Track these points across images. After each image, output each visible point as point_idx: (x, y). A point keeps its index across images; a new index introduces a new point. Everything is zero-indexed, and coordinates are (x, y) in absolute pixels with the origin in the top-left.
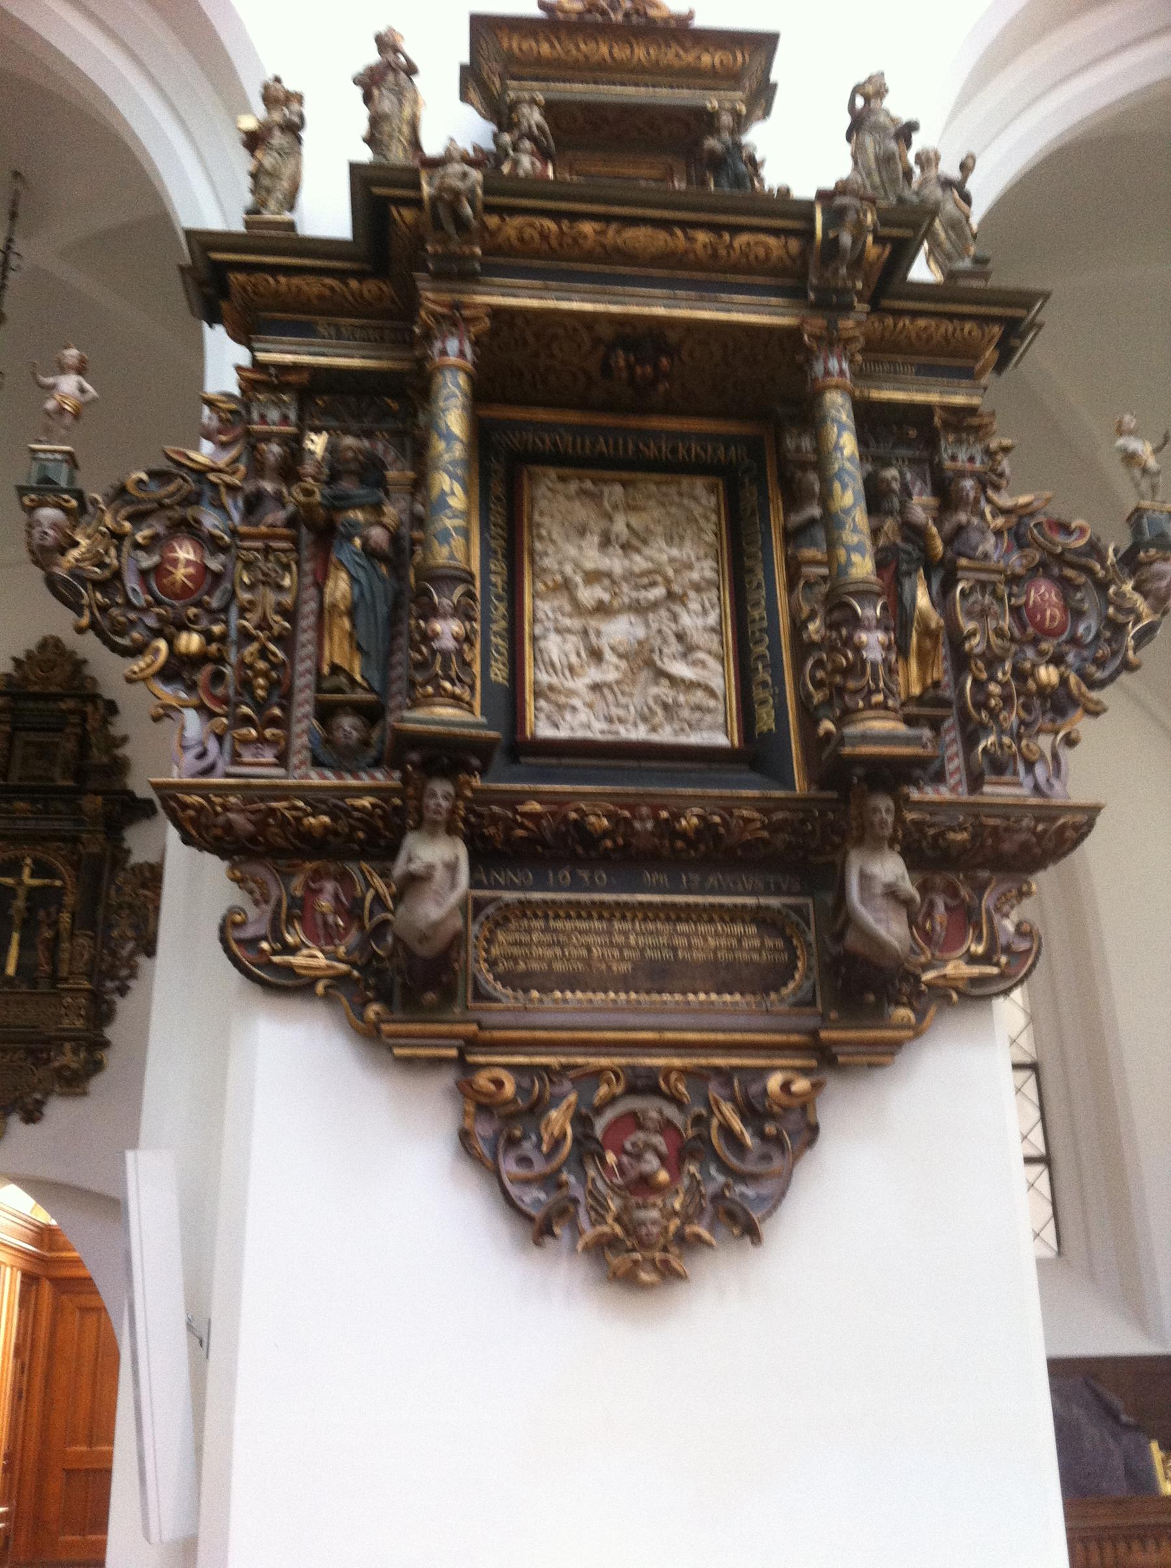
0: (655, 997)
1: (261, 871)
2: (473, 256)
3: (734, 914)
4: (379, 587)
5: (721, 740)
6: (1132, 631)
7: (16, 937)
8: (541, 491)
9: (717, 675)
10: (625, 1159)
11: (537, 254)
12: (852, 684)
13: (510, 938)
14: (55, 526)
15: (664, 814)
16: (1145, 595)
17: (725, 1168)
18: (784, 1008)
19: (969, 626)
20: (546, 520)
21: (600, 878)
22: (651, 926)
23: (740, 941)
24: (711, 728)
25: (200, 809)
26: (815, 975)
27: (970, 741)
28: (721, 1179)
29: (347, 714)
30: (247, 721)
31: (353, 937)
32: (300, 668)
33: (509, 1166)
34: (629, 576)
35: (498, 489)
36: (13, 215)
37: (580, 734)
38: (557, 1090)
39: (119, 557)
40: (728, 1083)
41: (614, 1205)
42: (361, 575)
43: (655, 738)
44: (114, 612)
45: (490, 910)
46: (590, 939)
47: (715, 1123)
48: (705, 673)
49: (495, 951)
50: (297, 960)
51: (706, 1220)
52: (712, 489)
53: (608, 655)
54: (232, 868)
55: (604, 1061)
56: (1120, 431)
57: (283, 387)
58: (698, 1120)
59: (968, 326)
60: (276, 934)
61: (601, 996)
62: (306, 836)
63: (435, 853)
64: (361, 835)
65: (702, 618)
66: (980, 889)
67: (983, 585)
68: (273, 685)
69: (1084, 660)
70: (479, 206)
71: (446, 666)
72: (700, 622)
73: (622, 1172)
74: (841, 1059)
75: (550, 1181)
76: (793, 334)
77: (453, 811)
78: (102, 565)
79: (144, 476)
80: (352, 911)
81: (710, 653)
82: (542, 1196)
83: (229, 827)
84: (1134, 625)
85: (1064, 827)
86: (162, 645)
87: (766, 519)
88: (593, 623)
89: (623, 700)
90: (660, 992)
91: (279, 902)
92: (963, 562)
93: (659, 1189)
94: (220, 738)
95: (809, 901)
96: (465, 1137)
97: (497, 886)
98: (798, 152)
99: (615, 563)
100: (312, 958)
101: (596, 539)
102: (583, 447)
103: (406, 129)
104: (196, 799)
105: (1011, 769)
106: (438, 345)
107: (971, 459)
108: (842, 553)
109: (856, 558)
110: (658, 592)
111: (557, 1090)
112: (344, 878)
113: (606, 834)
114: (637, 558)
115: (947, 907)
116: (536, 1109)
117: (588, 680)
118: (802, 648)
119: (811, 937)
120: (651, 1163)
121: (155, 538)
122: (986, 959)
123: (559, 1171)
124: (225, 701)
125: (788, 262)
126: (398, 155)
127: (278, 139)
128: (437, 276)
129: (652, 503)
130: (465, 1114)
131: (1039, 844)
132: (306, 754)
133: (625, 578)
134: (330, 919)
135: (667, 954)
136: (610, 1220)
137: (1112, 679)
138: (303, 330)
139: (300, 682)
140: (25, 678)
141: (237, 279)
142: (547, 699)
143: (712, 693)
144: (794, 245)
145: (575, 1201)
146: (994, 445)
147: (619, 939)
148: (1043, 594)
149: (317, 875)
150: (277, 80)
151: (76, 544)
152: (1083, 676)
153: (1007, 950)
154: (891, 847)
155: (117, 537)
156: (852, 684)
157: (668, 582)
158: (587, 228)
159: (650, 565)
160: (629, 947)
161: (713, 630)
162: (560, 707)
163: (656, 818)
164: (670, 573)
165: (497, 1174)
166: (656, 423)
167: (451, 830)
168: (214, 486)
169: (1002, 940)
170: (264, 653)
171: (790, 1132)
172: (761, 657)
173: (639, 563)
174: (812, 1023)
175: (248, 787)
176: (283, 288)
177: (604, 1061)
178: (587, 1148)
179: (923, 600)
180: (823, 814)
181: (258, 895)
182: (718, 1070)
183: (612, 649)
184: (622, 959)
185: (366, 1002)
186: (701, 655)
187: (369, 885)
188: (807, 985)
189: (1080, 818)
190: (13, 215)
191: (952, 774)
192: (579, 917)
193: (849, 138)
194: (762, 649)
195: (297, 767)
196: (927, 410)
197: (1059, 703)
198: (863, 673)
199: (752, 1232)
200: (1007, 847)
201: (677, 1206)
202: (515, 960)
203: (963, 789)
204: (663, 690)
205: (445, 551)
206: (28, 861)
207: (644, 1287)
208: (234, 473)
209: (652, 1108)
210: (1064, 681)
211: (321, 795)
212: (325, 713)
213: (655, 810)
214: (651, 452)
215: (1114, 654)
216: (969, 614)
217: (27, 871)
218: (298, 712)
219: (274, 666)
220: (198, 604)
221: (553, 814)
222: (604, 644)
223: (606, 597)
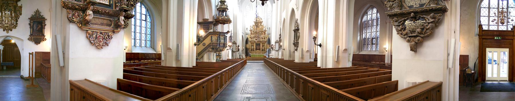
3: (108, 20)
80: (79, 16)
178: (96, 38)
209: (101, 35)
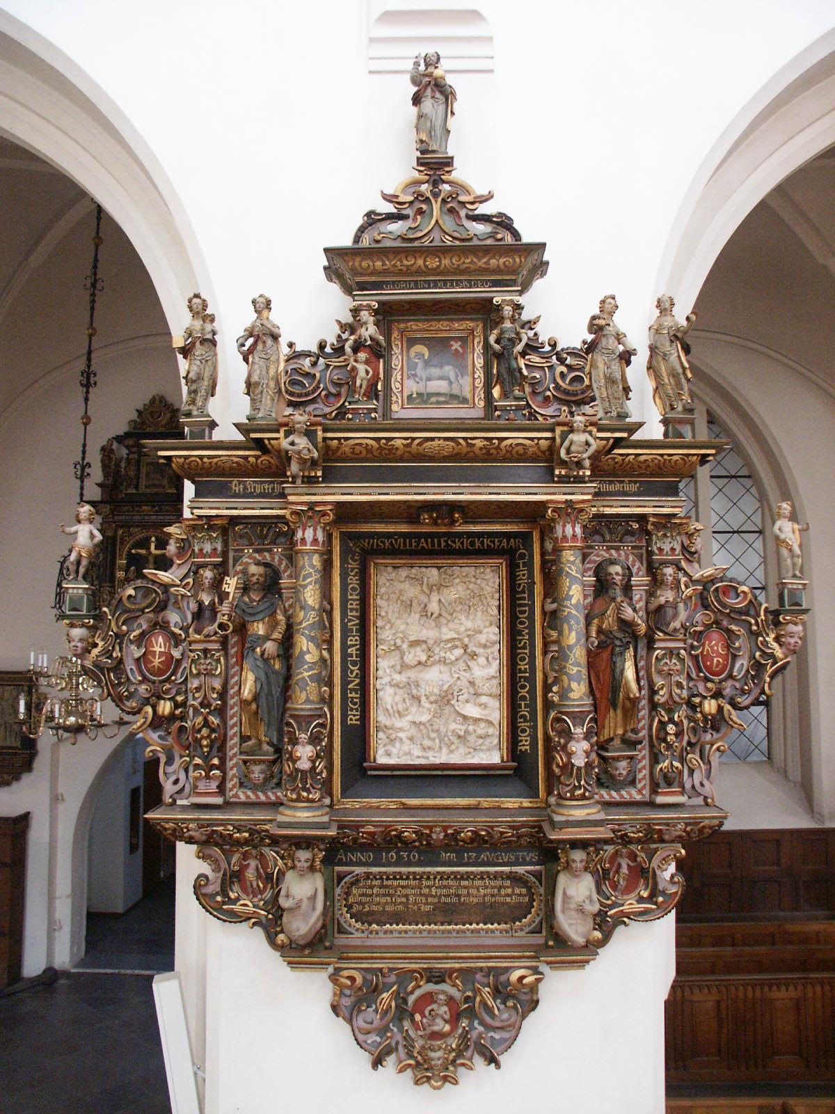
3: (496, 876)
5: (494, 758)
8: (382, 580)
9: (494, 711)
13: (360, 891)
15: (449, 832)
17: (482, 1023)
21: (414, 856)
23: (499, 891)
25: (175, 830)
28: (481, 1029)
34: (438, 642)
38: (387, 980)
39: (121, 650)
46: (408, 891)
47: (478, 999)
49: (351, 900)
57: (211, 528)
60: (224, 893)
65: (488, 670)
71: (304, 781)
73: (424, 1029)
75: (382, 1031)
76: (543, 505)
78: (110, 657)
84: (773, 664)
85: (704, 827)
86: (149, 709)
97: (351, 863)
99: (428, 633)
102: (411, 545)
103: (272, 384)
109: (574, 685)
110: (458, 652)
111: (387, 980)
117: (409, 718)
127: (199, 350)
132: (235, 780)
134: (255, 885)
135: (454, 900)
140: (143, 423)
143: (490, 723)
147: (426, 891)
151: (96, 645)
155: (119, 637)
157: (465, 647)
159: (455, 636)
160: (432, 896)
164: (466, 640)
169: (660, 887)
170: (206, 723)
172: (523, 698)
177: (413, 966)
178: (402, 1012)
179: (630, 673)
184: (427, 904)
186: (484, 699)
188: (538, 920)
189: (716, 822)
192: (401, 878)
195: (231, 790)
197: (717, 722)
201: (454, 1046)
202: (363, 904)
203: (646, 792)
205: (303, 696)
206: (153, 539)
210: (720, 709)
213: (445, 829)
214: (457, 545)
216: (660, 672)
217: (153, 546)
223: (423, 658)
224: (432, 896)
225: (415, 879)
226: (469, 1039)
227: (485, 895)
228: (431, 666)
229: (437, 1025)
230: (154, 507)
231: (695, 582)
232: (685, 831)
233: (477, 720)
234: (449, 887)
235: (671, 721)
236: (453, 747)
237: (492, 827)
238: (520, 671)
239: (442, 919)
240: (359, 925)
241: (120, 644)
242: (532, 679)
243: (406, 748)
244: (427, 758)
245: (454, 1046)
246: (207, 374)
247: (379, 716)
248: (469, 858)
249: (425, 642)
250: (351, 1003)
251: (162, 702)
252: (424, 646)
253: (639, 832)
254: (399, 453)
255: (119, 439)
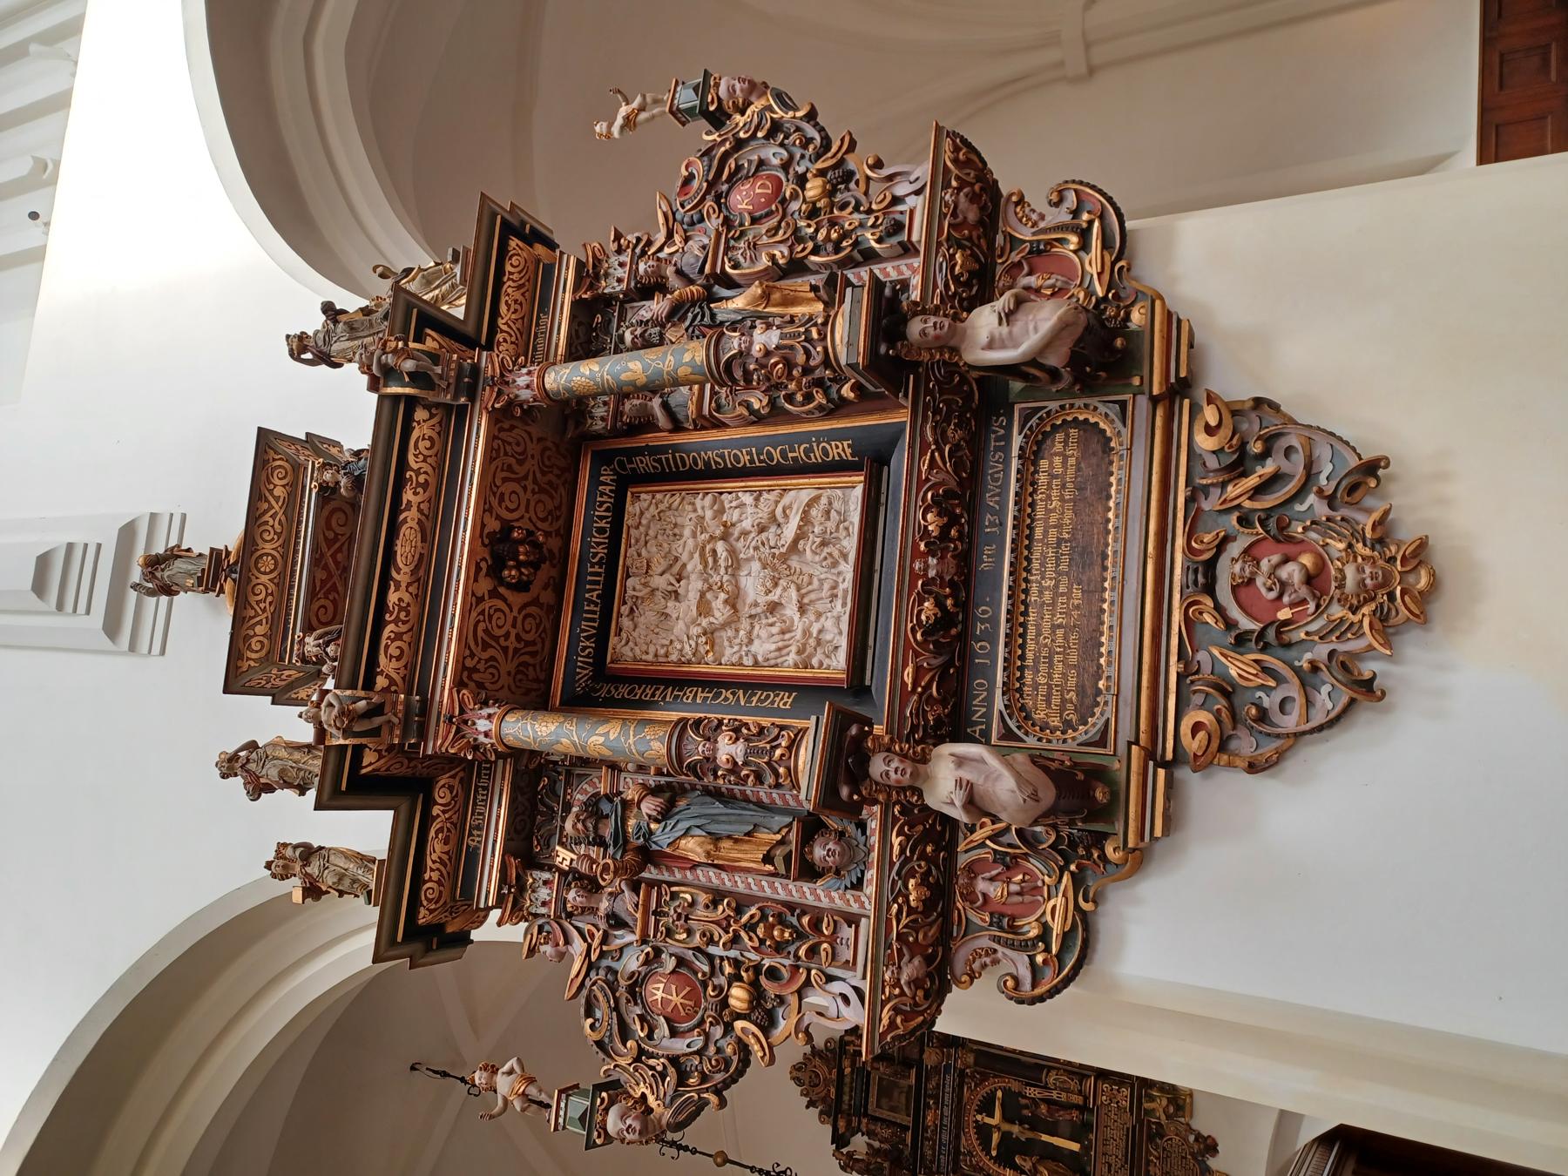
0: (1109, 562)
1: (961, 956)
2: (408, 704)
3: (1027, 481)
4: (694, 810)
6: (779, 113)
7: (1045, 1138)
8: (626, 651)
9: (800, 492)
10: (1286, 599)
11: (414, 645)
12: (800, 358)
13: (1042, 705)
14: (623, 1117)
16: (747, 104)
17: (1299, 495)
18: (1126, 433)
19: (764, 261)
20: (652, 649)
21: (984, 612)
22: (1035, 565)
23: (1056, 477)
24: (846, 502)
25: (895, 1009)
26: (1093, 401)
27: (870, 256)
28: (1312, 499)
29: (811, 853)
30: (813, 951)
31: (1034, 865)
32: (768, 892)
33: (1290, 722)
34: (705, 575)
35: (624, 691)
36: (445, 1074)
37: (845, 627)
38: (1206, 668)
39: (657, 1057)
40: (1205, 490)
41: (1337, 611)
42: (683, 826)
43: (852, 556)
44: (706, 1067)
45: (1012, 724)
46: (1046, 626)
47: (1247, 504)
48: (795, 507)
49: (1055, 722)
50: (1057, 928)
51: (1360, 517)
52: (636, 497)
53: (774, 596)
54: (959, 983)
55: (1177, 617)
56: (609, 135)
57: (521, 887)
58: (1244, 521)
59: (508, 268)
60: (1026, 946)
61: (1106, 617)
62: (928, 905)
63: (946, 778)
64: (929, 849)
65: (745, 505)
66: (1013, 242)
67: (728, 249)
68: (781, 920)
69: (803, 157)
70: (361, 693)
72: (750, 510)
73: (1304, 602)
74: (1183, 375)
75: (1308, 678)
76: (497, 417)
77: (903, 756)
78: (663, 1075)
79: (590, 1021)
81: (777, 502)
82: (1325, 689)
83: (915, 983)
85: (955, 161)
87: (663, 449)
88: (745, 611)
89: (816, 583)
90: (1104, 556)
91: (995, 939)
92: (707, 269)
93: (1321, 566)
94: (831, 979)
95: (1017, 407)
96: (1253, 768)
97: (988, 716)
98: (344, 408)
99: (693, 587)
100: (1056, 910)
101: (671, 604)
102: (594, 612)
103: (297, 755)
104: (886, 1015)
105: (898, 217)
106: (482, 738)
107: (622, 265)
108: (682, 371)
109: (687, 358)
110: (720, 547)
111: (1206, 668)
112: (972, 870)
113: (939, 604)
114: (689, 567)
115: (1030, 274)
116: (1227, 690)
118: (776, 414)
119: (1053, 405)
120: (1292, 572)
121: (642, 1018)
122: (1084, 234)
123: (1297, 671)
124: (795, 969)
125: (435, 420)
126: (315, 765)
128: (423, 735)
129: (644, 552)
130: (1229, 765)
131: (972, 185)
133: (706, 580)
134: (1014, 888)
136: (1356, 618)
137: (821, 130)
138: (473, 858)
139: (782, 896)
140: (824, 1100)
141: (423, 917)
142: (810, 656)
143: (816, 499)
144: (420, 414)
145: (1332, 654)
146: (614, 247)
147: (1047, 596)
148: (742, 200)
149: (970, 897)
150: (268, 866)
152: (818, 156)
153: (1076, 213)
154: (963, 321)
156: (800, 358)
158: (393, 597)
159: (697, 555)
160: (1056, 586)
161: (757, 499)
162: (819, 642)
163: (924, 555)
164: (705, 537)
165: (1298, 735)
166: (576, 547)
167: (924, 759)
168: (602, 955)
169: (1067, 218)
170: (750, 928)
171: (1257, 431)
172: (783, 454)
173: (694, 565)
174: (1143, 401)
175: (875, 960)
176: (435, 875)
177: (1177, 617)
180: (928, 392)
181: (988, 960)
182: (1189, 501)
183: (768, 592)
184: (1069, 595)
185: (1103, 857)
187: (983, 845)
188: (1102, 409)
189: (947, 144)
190: (445, 1074)
191: (900, 273)
193: (339, 365)
194: (777, 455)
196: (576, 304)
198: (791, 347)
199: (1372, 468)
200: (972, 216)
201: (1342, 546)
202: (1064, 701)
204: (807, 546)
205: (656, 745)
206: (979, 1117)
207: (1435, 583)
208: (592, 936)
210: (822, 173)
211: (887, 886)
212: (810, 872)
213: (916, 554)
214: (602, 551)
215: (798, 129)
217: (988, 1120)
218: (810, 900)
219: (764, 917)
220: (705, 985)
221: (916, 654)
222: (762, 600)
223: (723, 596)
224: (1056, 586)
225: (1025, 614)
226: (1328, 519)
227: (1062, 499)
228: (737, 586)
229: (1290, 576)
230: (927, 1106)
231: (670, 235)
232: (959, 189)
233: (806, 518)
234: (1044, 556)
235: (813, 238)
236: (836, 554)
237: (920, 483)
238: (752, 461)
239: (1097, 569)
240: (1097, 710)
241: (651, 1056)
242: (759, 443)
243: (829, 624)
244: (846, 591)
245: (1342, 546)
246: (342, 862)
247: (788, 666)
248: (992, 524)
249: (703, 594)
250: (1248, 735)
251: (732, 1002)
252: (709, 596)
253: (952, 257)
254: (407, 598)
255: (839, 1140)
